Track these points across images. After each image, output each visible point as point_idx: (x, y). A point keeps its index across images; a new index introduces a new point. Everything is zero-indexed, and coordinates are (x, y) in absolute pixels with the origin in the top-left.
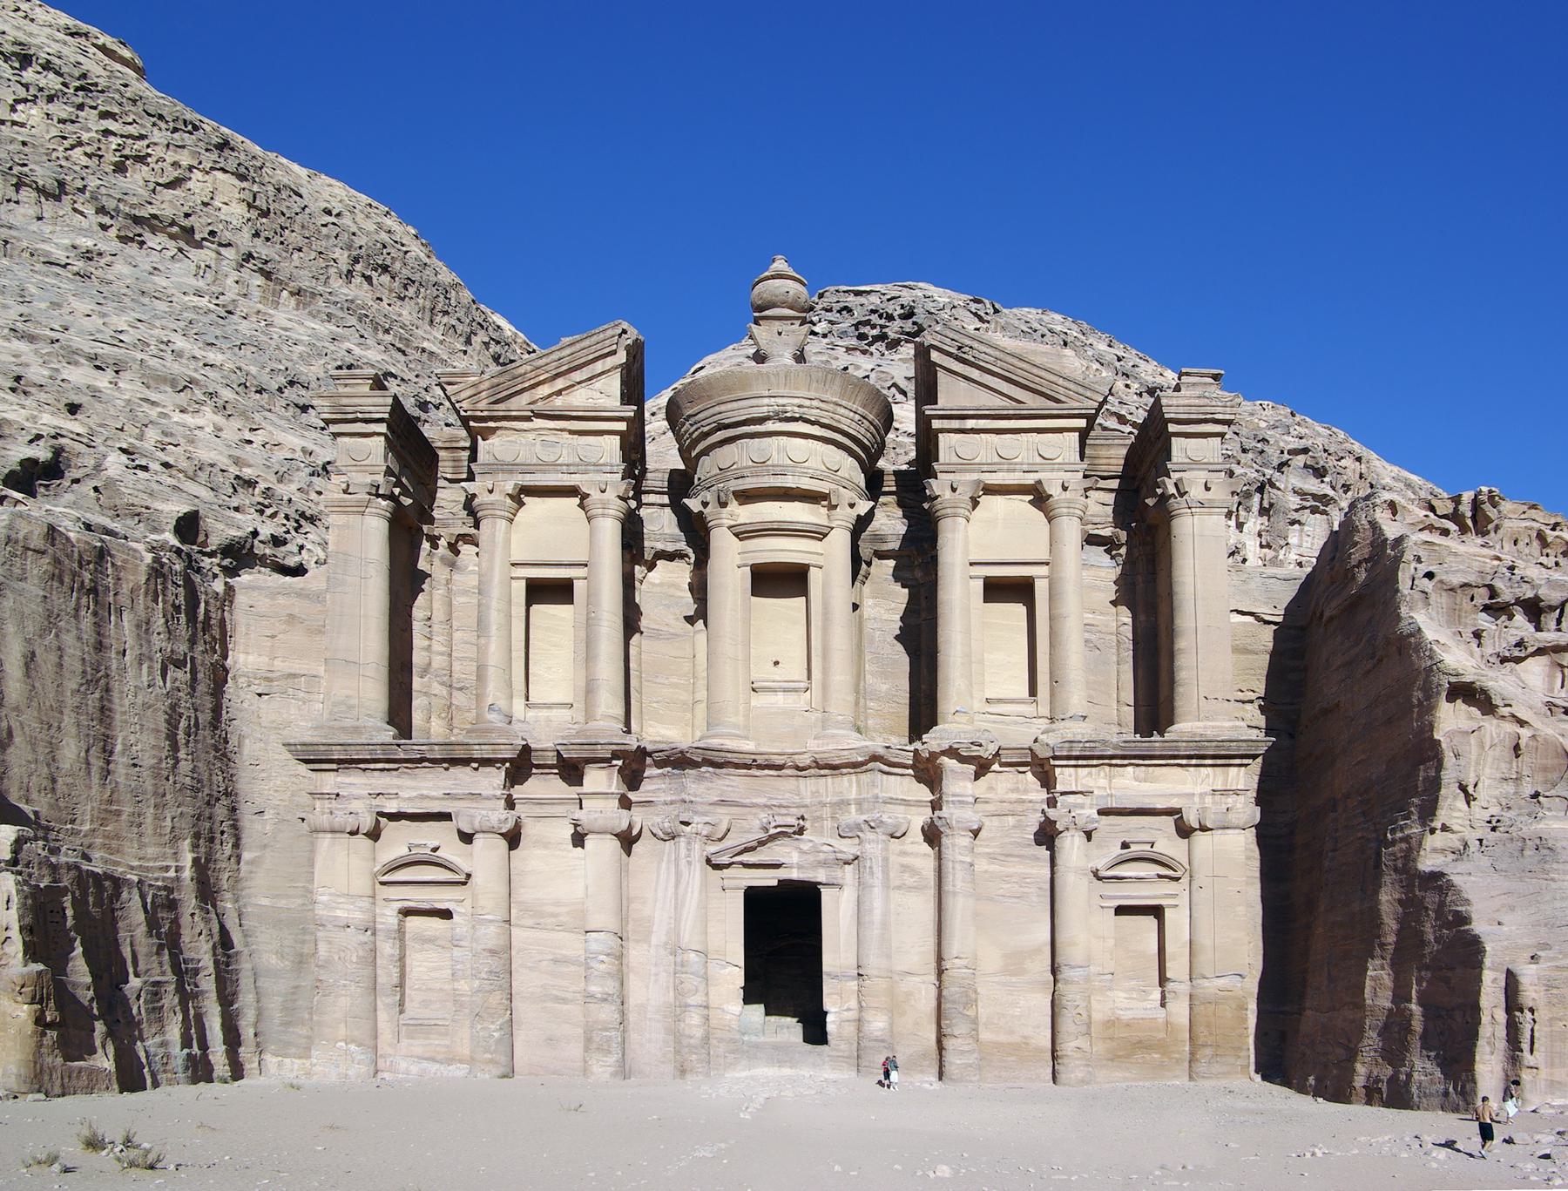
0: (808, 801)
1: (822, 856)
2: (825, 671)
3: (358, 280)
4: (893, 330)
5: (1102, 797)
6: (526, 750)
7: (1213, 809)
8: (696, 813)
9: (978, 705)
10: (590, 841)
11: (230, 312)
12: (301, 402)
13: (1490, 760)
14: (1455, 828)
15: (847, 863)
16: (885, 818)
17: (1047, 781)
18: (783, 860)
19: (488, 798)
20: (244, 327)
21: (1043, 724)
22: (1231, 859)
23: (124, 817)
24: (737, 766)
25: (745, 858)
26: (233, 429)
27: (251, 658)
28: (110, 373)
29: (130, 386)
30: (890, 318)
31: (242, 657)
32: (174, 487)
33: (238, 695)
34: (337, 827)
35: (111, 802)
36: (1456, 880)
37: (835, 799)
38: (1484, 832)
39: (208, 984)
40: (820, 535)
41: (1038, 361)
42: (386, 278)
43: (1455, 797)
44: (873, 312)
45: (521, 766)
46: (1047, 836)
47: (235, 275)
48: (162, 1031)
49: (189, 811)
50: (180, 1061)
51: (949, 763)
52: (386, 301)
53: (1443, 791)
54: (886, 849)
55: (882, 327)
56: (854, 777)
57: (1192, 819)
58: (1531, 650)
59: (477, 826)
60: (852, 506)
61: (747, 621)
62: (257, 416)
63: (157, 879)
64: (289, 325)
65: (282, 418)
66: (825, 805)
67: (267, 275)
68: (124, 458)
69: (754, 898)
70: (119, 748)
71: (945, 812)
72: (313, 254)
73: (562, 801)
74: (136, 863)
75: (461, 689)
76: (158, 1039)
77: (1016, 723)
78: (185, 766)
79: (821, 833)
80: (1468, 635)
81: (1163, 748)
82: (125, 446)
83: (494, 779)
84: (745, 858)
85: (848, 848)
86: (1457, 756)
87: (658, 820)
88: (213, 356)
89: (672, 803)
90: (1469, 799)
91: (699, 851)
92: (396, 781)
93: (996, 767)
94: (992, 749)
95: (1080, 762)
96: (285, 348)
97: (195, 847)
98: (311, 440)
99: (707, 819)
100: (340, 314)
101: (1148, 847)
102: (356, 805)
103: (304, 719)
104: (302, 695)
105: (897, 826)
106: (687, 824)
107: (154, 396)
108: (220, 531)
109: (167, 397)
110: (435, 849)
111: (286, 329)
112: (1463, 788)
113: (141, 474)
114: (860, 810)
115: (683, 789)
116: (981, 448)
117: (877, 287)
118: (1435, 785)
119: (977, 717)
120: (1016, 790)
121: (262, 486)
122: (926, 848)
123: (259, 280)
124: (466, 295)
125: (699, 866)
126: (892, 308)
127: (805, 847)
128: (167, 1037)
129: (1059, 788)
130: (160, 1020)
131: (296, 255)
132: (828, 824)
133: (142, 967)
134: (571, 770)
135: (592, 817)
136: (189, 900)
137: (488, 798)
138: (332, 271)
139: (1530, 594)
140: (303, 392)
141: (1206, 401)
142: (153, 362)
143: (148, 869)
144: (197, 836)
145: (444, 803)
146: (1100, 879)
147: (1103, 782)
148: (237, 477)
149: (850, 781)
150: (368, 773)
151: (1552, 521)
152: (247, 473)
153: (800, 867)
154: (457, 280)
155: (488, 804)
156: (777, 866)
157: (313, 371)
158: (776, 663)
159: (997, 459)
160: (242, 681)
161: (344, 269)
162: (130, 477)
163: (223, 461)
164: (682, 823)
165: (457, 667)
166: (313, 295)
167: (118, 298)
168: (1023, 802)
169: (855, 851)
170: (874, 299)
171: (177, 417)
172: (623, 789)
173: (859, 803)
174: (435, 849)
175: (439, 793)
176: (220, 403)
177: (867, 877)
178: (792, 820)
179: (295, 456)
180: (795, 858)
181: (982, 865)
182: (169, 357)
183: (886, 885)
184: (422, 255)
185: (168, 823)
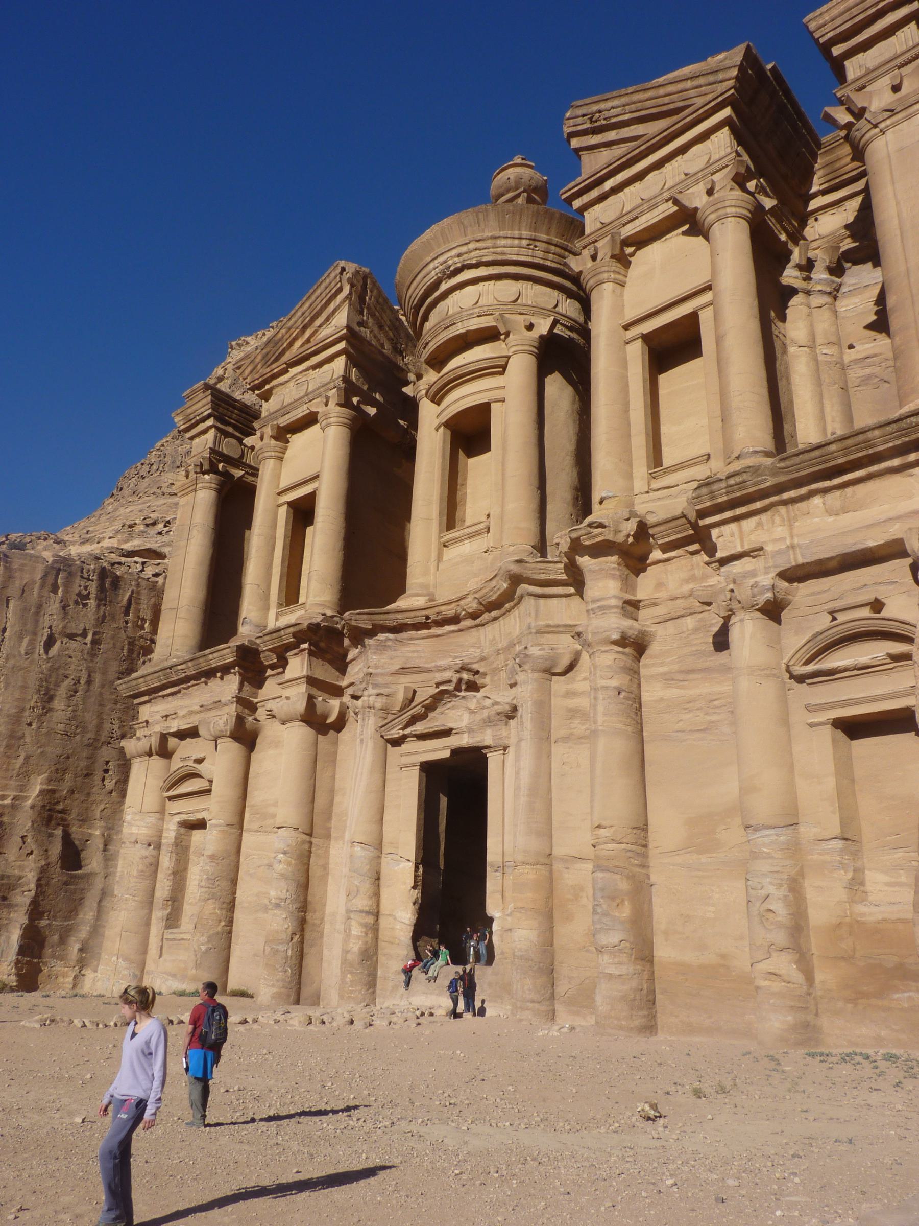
5: (780, 552)
24: (417, 627)
25: (419, 728)
40: (499, 368)
69: (429, 769)
81: (846, 451)
93: (656, 555)
95: (739, 511)
101: (866, 612)
110: (199, 761)
120: (693, 578)
146: (801, 679)
147: (780, 531)
153: (470, 730)
174: (199, 761)
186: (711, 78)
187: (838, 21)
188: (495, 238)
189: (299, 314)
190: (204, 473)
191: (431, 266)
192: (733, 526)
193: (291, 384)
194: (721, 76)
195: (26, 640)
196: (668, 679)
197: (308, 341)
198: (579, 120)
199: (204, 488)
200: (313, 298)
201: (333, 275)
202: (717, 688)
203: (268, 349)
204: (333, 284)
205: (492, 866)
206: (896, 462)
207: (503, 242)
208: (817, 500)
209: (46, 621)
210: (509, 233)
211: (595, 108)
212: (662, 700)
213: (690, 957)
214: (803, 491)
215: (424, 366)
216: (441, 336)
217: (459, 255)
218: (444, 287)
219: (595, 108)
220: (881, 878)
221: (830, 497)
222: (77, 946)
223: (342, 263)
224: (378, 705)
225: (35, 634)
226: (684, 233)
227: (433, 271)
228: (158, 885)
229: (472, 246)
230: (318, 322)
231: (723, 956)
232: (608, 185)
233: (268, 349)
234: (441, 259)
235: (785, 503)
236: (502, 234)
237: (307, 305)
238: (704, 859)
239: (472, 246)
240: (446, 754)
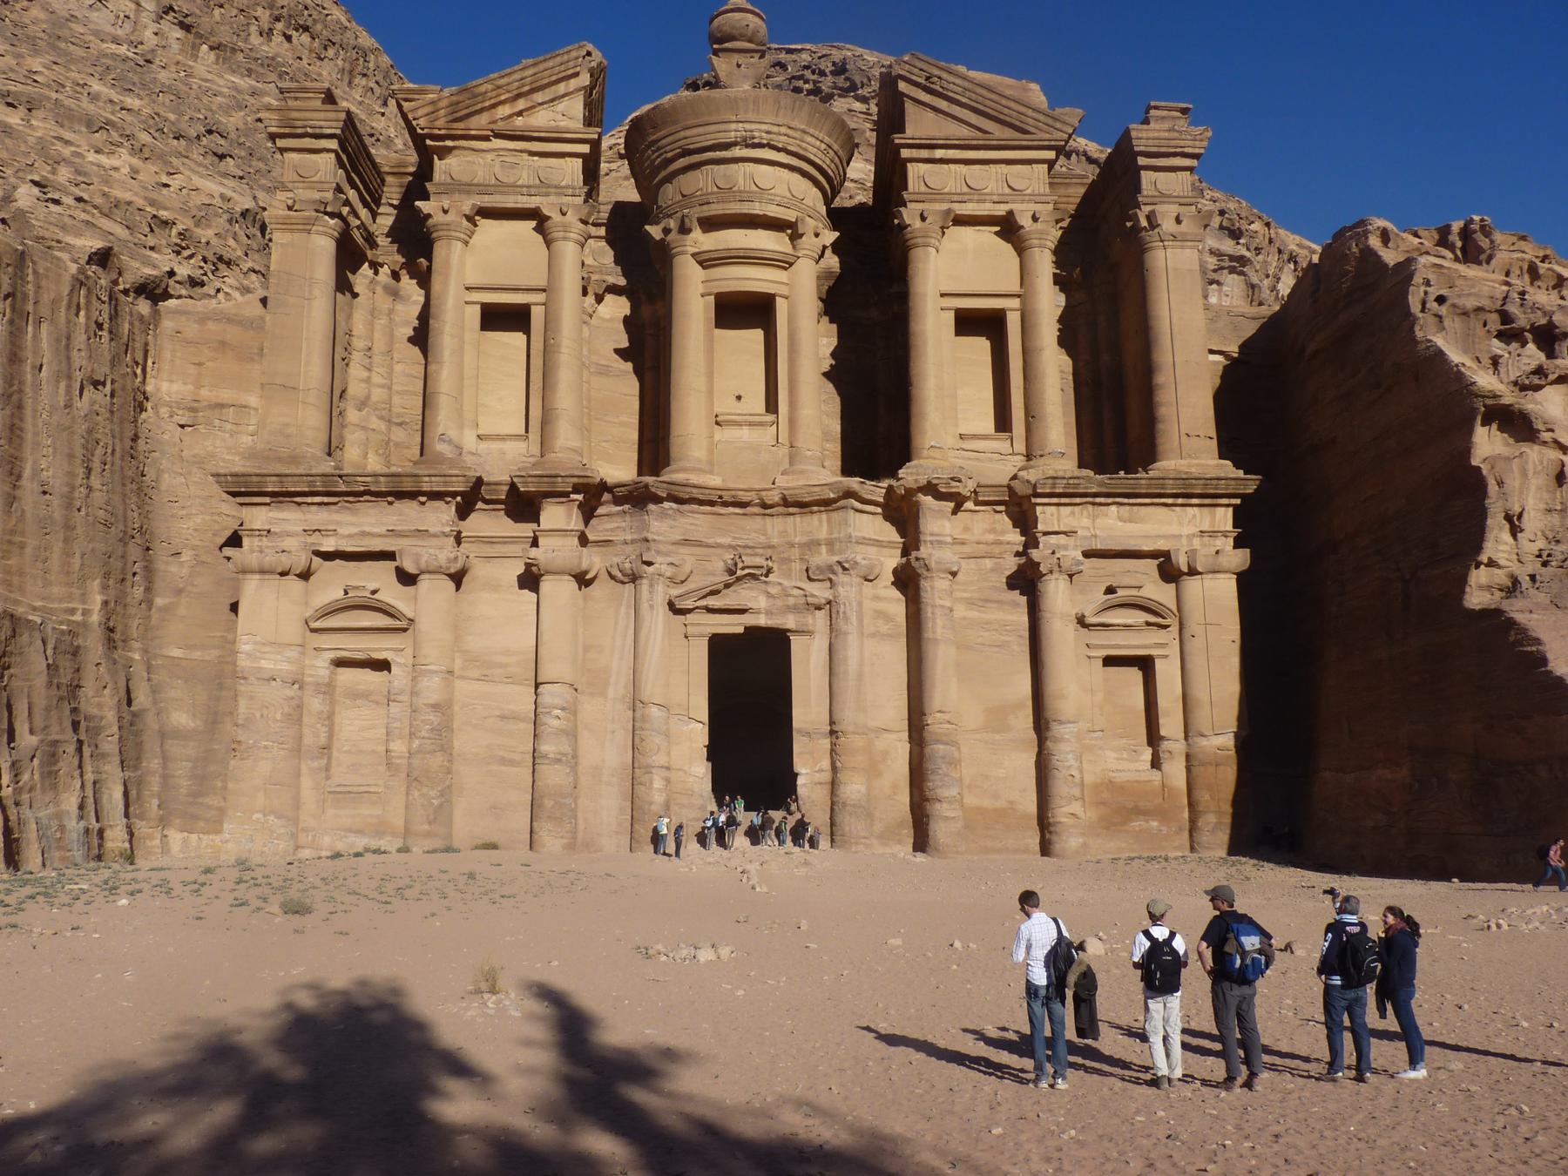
0: (775, 541)
1: (791, 601)
2: (793, 405)
3: (278, 38)
4: (826, 84)
5: (1085, 537)
6: (479, 482)
7: (1205, 552)
8: (658, 552)
9: (951, 441)
10: (546, 585)
11: (149, 61)
12: (220, 151)
13: (1533, 488)
14: (1502, 562)
15: (819, 608)
16: (859, 559)
17: (1023, 518)
18: (750, 605)
19: (435, 536)
20: (163, 76)
21: (1019, 461)
22: (1216, 600)
23: (28, 550)
26: (150, 172)
27: (175, 387)
28: (22, 110)
29: (42, 126)
30: (822, 73)
31: (165, 386)
32: (88, 222)
33: (160, 424)
34: (267, 567)
35: (13, 532)
36: (1519, 617)
37: (804, 539)
38: (1533, 566)
39: (110, 745)
40: (786, 264)
41: (1008, 92)
42: (305, 38)
43: (1501, 529)
44: (806, 67)
45: (469, 499)
46: (1026, 580)
47: (153, 27)
48: (56, 802)
49: (101, 547)
50: (74, 836)
51: (927, 500)
52: (305, 62)
53: (1489, 522)
54: (860, 592)
55: (815, 82)
56: (824, 516)
57: (1182, 562)
58: (1552, 377)
59: (423, 565)
60: (817, 235)
61: (710, 351)
62: (174, 160)
63: (61, 623)
64: (210, 77)
65: (200, 165)
66: (792, 546)
67: (187, 28)
68: (36, 190)
70: (27, 473)
71: (924, 552)
72: (234, 12)
73: (514, 540)
74: (39, 604)
75: (400, 424)
76: (51, 810)
77: (991, 460)
78: (98, 497)
79: (789, 577)
80: (1486, 361)
82: (36, 178)
83: (441, 516)
84: (712, 602)
85: (820, 592)
86: (1500, 484)
87: (616, 560)
88: (130, 101)
89: (633, 542)
90: (1515, 531)
91: (662, 593)
92: (335, 517)
94: (971, 485)
95: (1063, 500)
96: (205, 99)
97: (105, 587)
98: (228, 188)
99: (670, 560)
100: (260, 69)
102: (290, 543)
103: (230, 449)
104: (228, 426)
105: (871, 568)
106: (649, 564)
107: (68, 136)
108: (137, 269)
109: (80, 138)
111: (206, 81)
112: (1508, 518)
113: (53, 208)
114: (831, 551)
115: (646, 527)
116: (948, 178)
117: (808, 46)
118: (1481, 515)
119: (951, 453)
120: (992, 531)
121: (180, 227)
122: (896, 594)
123: (179, 33)
124: (386, 60)
125: (662, 611)
126: (827, 66)
127: (773, 590)
128: (63, 807)
129: (1041, 527)
130: (54, 787)
131: (217, 11)
132: (797, 567)
133: (39, 722)
134: (523, 505)
135: (550, 555)
136: (94, 646)
137: (435, 536)
138: (253, 29)
139: (1544, 321)
140: (222, 142)
141: (1176, 135)
142: (68, 102)
143: (51, 612)
144: (107, 575)
145: (387, 540)
147: (1086, 522)
148: (155, 216)
149: (820, 521)
150: (304, 508)
151: (1541, 254)
152: (164, 214)
153: (769, 613)
154: (376, 45)
155: (435, 541)
156: (742, 611)
157: (232, 121)
158: (739, 398)
159: (966, 189)
160: (164, 411)
161: (266, 27)
162: (41, 210)
163: (140, 202)
164: (645, 563)
165: (396, 400)
166: (234, 50)
167: (32, 41)
168: (999, 543)
169: (828, 595)
170: (805, 57)
171: (92, 157)
172: (581, 527)
173: (830, 544)
175: (382, 530)
176: (137, 146)
177: (841, 622)
178: (759, 561)
179: (214, 202)
180: (762, 602)
181: (961, 611)
182: (85, 99)
183: (861, 633)
184: (343, 19)
185: (77, 560)
186: (1050, 121)
187: (1150, 142)
188: (804, 132)
189: (517, 76)
190: (326, 213)
191: (733, 126)
192: (1053, 508)
193: (490, 156)
194: (1058, 125)
195: (62, 385)
196: (970, 603)
197: (520, 114)
198: (916, 71)
199: (325, 234)
200: (541, 67)
201: (574, 54)
202: (1010, 617)
203: (460, 98)
204: (571, 64)
205: (799, 731)
206: (1170, 501)
207: (810, 139)
208: (1114, 508)
209: (79, 359)
210: (816, 133)
211: (936, 72)
212: (964, 618)
213: (988, 803)
214: (1110, 500)
215: (695, 223)
216: (732, 205)
217: (768, 132)
218: (737, 152)
219: (936, 72)
220: (1113, 755)
221: (1122, 508)
222: (155, 802)
223: (590, 47)
224: (668, 574)
225: (69, 377)
226: (996, 233)
227: (734, 131)
228: (306, 731)
229: (783, 130)
231: (1011, 802)
232: (939, 153)
233: (460, 98)
234: (748, 126)
235: (1094, 504)
236: (811, 131)
237: (531, 71)
238: (997, 737)
239: (783, 130)
240: (741, 630)
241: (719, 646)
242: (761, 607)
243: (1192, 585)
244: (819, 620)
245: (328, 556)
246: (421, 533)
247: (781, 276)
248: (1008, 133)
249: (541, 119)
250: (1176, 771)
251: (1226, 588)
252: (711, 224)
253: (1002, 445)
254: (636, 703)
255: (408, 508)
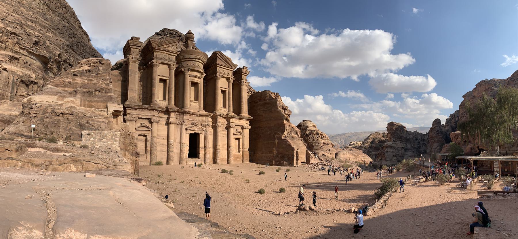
40: (200, 78)
180: (196, 129)
218: (197, 60)
227: (197, 57)
230: (170, 45)
241: (191, 135)
242: (196, 130)
243: (245, 130)
244: (203, 132)
245: (139, 118)
246: (154, 116)
247: (199, 80)
248: (228, 65)
249: (170, 49)
250: (241, 152)
251: (248, 130)
252: (192, 70)
253: (224, 109)
254: (181, 143)
255: (152, 112)
